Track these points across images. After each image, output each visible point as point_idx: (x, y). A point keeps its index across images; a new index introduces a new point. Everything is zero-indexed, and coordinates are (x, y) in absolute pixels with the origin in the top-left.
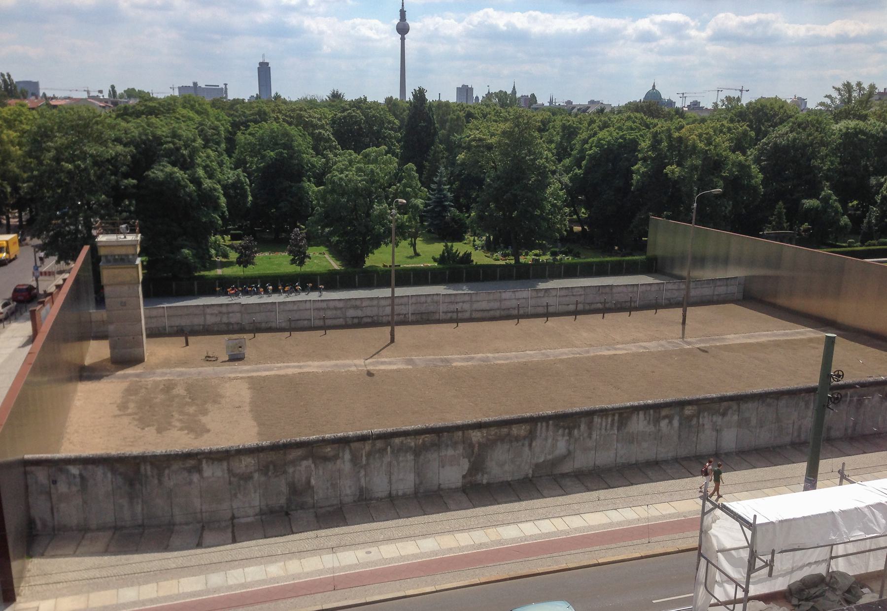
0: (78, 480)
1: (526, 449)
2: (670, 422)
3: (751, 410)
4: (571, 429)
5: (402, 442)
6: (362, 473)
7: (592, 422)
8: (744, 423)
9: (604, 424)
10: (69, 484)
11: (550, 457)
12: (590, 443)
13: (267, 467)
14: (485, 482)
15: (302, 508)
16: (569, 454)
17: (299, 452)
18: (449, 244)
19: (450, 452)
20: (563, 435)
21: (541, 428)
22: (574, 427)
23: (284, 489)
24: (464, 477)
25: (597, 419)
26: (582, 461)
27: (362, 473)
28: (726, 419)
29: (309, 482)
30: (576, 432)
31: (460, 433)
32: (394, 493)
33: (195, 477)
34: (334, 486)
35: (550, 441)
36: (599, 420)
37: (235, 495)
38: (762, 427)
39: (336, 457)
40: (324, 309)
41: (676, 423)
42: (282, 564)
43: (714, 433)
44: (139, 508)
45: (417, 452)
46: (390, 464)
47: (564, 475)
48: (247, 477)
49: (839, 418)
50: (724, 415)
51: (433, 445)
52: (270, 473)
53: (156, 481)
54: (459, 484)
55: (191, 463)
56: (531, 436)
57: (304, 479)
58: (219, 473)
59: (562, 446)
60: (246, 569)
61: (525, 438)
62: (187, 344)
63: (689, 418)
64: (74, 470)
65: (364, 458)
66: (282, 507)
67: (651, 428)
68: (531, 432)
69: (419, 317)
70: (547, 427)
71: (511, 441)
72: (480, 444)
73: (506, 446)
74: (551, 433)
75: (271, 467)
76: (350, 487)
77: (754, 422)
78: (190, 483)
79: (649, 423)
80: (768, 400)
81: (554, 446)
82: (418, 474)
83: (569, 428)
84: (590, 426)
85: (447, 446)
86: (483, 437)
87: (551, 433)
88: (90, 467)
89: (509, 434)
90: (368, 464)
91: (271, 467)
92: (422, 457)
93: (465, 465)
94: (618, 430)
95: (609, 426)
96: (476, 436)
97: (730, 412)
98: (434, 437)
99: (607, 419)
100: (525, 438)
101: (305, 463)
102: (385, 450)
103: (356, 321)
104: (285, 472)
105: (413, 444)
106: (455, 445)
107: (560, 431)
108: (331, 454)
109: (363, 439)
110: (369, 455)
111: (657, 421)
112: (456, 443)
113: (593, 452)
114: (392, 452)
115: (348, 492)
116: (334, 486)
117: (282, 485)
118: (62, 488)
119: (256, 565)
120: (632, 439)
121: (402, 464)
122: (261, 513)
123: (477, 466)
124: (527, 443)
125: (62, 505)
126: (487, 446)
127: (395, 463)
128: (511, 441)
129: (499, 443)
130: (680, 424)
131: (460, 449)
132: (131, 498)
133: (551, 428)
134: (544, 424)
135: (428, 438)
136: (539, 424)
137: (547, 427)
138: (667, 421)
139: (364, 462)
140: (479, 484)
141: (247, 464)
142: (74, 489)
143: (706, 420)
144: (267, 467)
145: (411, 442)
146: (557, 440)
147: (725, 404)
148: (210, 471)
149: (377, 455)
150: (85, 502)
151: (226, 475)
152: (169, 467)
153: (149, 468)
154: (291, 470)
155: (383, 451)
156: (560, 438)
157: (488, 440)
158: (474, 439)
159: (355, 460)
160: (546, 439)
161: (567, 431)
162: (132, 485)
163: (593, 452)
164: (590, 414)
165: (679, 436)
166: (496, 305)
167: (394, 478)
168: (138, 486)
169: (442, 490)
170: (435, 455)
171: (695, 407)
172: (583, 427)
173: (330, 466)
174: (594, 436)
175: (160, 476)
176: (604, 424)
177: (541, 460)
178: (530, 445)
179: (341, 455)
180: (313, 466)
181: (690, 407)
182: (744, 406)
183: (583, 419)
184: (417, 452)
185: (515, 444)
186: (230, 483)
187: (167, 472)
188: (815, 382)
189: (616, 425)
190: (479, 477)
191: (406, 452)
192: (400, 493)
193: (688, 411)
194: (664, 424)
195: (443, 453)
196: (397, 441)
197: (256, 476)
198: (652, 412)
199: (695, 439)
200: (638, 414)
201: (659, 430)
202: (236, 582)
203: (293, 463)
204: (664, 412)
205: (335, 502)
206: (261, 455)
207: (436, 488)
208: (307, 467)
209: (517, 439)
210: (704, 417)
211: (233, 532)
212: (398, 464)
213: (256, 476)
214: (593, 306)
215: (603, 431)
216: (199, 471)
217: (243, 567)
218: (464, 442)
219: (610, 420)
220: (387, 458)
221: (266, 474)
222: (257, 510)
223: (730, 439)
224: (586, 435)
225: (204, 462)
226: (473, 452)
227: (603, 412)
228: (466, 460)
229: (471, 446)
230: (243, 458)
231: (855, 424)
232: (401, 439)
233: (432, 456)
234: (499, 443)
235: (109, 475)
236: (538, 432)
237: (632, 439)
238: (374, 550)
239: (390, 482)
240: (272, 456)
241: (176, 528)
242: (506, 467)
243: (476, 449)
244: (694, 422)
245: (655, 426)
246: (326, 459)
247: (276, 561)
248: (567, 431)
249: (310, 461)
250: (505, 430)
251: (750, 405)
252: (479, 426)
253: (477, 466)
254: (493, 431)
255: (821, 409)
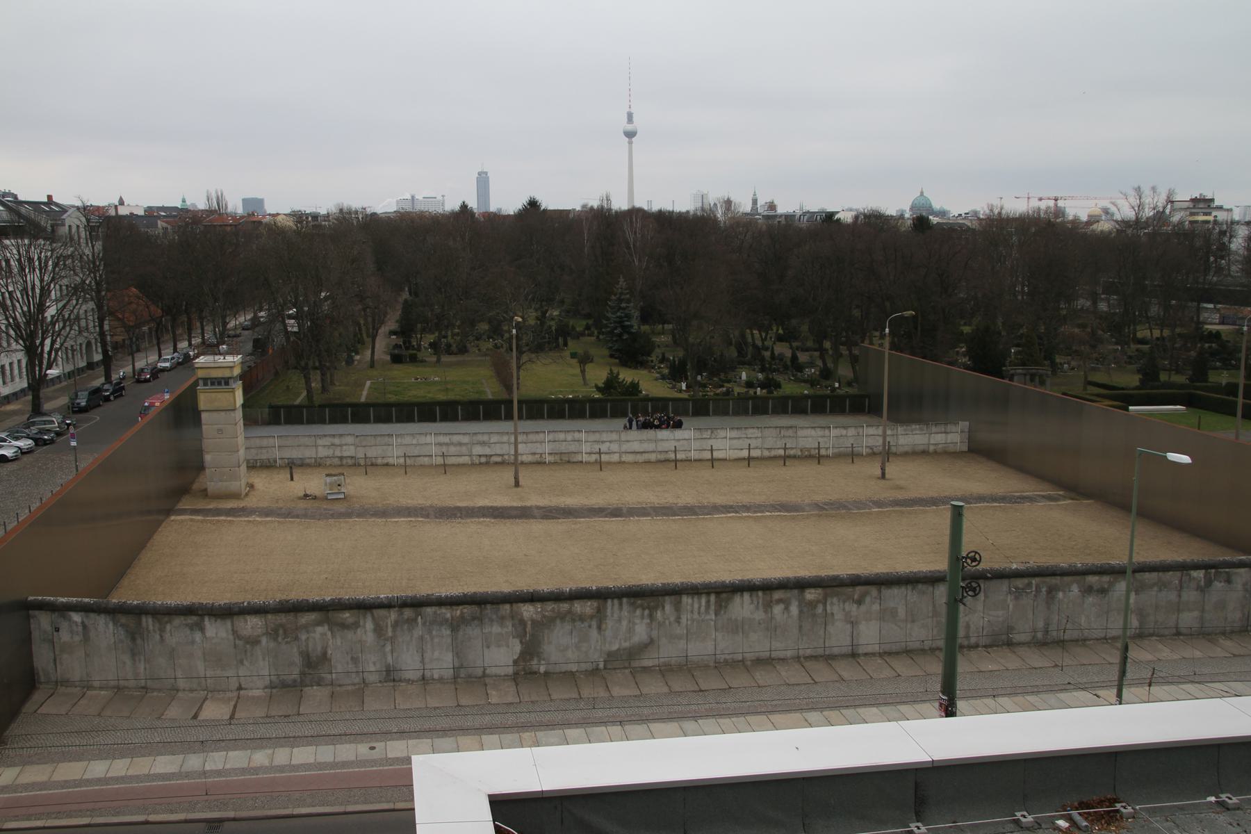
0: (80, 628)
1: (594, 633)
2: (787, 608)
3: (895, 597)
4: (652, 610)
5: (435, 613)
6: (388, 648)
7: (680, 602)
8: (887, 615)
9: (696, 606)
10: (72, 632)
11: (626, 645)
12: (679, 631)
13: (276, 631)
14: (542, 669)
15: (319, 685)
16: (650, 643)
17: (313, 616)
18: (615, 370)
19: (496, 629)
20: (642, 617)
21: (611, 606)
22: (656, 608)
23: (297, 659)
24: (515, 662)
25: (686, 600)
26: (668, 652)
27: (388, 648)
28: (863, 608)
29: (325, 654)
30: (659, 613)
31: (507, 607)
32: (428, 674)
33: (198, 636)
34: (355, 660)
35: (625, 623)
36: (690, 601)
37: (241, 662)
38: (913, 621)
39: (356, 625)
40: (447, 444)
41: (794, 609)
42: (270, 751)
43: (849, 626)
44: (142, 666)
45: (455, 626)
46: (422, 638)
47: (645, 669)
48: (254, 642)
49: (978, 616)
50: (859, 602)
51: (474, 619)
52: (280, 639)
53: (158, 637)
54: (510, 670)
55: (195, 618)
56: (600, 616)
57: (319, 649)
58: (223, 634)
59: (641, 631)
60: (230, 753)
61: (592, 617)
62: (292, 479)
63: (812, 605)
64: (76, 617)
65: (390, 629)
66: (295, 681)
67: (760, 615)
68: (599, 611)
69: (557, 458)
70: (621, 604)
71: (573, 621)
72: (534, 622)
73: (568, 627)
74: (625, 613)
75: (281, 632)
76: (374, 663)
77: (902, 612)
78: (193, 642)
79: (757, 608)
80: (920, 586)
81: (631, 630)
82: (457, 654)
83: (649, 608)
84: (678, 607)
85: (491, 620)
86: (537, 613)
87: (625, 613)
88: (92, 615)
89: (569, 612)
90: (392, 640)
91: (281, 632)
92: (461, 633)
93: (517, 648)
94: (716, 615)
95: (703, 609)
96: (528, 611)
97: (868, 599)
98: (475, 608)
99: (699, 599)
100: (592, 617)
101: (319, 629)
102: (415, 620)
103: (483, 460)
104: (297, 638)
105: (448, 615)
106: (502, 619)
107: (638, 612)
108: (351, 620)
109: (388, 605)
110: (395, 625)
111: (768, 606)
112: (503, 618)
113: (683, 642)
114: (424, 624)
115: (372, 669)
116: (355, 660)
117: (292, 653)
118: (65, 636)
119: (244, 748)
120: (737, 627)
121: (436, 640)
122: (272, 686)
123: (530, 650)
124: (594, 623)
125: (65, 656)
126: (541, 625)
127: (427, 637)
128: (573, 621)
129: (558, 621)
130: (801, 612)
131: (509, 624)
132: (134, 654)
133: (625, 607)
134: (616, 601)
135: (467, 610)
136: (609, 601)
137: (621, 604)
138: (781, 606)
139: (390, 634)
140: (535, 673)
141: (252, 625)
142: (77, 638)
143: (835, 607)
144: (276, 631)
145: (447, 613)
146: (634, 624)
147: (859, 589)
148: (216, 631)
149: (406, 627)
150: (87, 655)
151: (231, 637)
152: (170, 622)
153: (150, 620)
154: (303, 637)
155: (412, 622)
156: (637, 621)
157: (544, 616)
158: (526, 615)
159: (379, 630)
160: (620, 620)
161: (647, 612)
162: (133, 639)
163: (683, 642)
164: (675, 592)
165: (800, 627)
166: (651, 447)
167: (428, 656)
168: (139, 641)
169: (489, 676)
170: (477, 631)
171: (820, 591)
172: (668, 607)
173: (350, 635)
174: (684, 620)
175: (162, 630)
176: (696, 606)
177: (615, 647)
178: (599, 628)
179: (362, 623)
180: (329, 634)
181: (813, 591)
182: (888, 592)
183: (667, 598)
184: (455, 626)
185: (578, 624)
186: (235, 646)
187: (168, 627)
188: (940, 564)
189: (713, 607)
190: (535, 662)
191: (441, 624)
192: (436, 676)
193: (810, 595)
194: (778, 609)
195: (486, 631)
196: (429, 610)
197: (264, 640)
198: (760, 593)
199: (822, 632)
200: (742, 596)
201: (772, 618)
202: (214, 768)
203: (306, 628)
204: (777, 595)
205: (357, 680)
206: (269, 616)
207: (479, 672)
208: (323, 634)
209: (582, 618)
210: (832, 604)
211: (235, 707)
212: (432, 639)
213: (264, 640)
214: (773, 453)
215: (696, 616)
216: (202, 629)
217: (227, 749)
218: (513, 618)
219: (704, 600)
220: (418, 631)
221: (275, 639)
222: (267, 683)
223: (870, 635)
224: (672, 619)
225: (206, 619)
226: (525, 629)
227: (694, 590)
228: (517, 641)
229: (522, 622)
230: (248, 618)
231: (1047, 625)
232: (434, 609)
233: (473, 631)
234: (558, 621)
235: (111, 625)
236: (609, 611)
237: (737, 627)
238: (379, 746)
239: (423, 661)
240: (282, 619)
241: (180, 694)
242: (570, 654)
243: (529, 628)
244: (820, 609)
245: (766, 612)
246: (344, 626)
247: (262, 748)
248: (647, 612)
249: (326, 627)
250: (565, 606)
251: (895, 591)
252: (533, 598)
253: (530, 650)
254: (550, 606)
255: (954, 603)
